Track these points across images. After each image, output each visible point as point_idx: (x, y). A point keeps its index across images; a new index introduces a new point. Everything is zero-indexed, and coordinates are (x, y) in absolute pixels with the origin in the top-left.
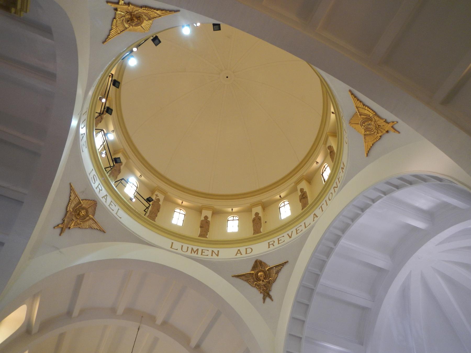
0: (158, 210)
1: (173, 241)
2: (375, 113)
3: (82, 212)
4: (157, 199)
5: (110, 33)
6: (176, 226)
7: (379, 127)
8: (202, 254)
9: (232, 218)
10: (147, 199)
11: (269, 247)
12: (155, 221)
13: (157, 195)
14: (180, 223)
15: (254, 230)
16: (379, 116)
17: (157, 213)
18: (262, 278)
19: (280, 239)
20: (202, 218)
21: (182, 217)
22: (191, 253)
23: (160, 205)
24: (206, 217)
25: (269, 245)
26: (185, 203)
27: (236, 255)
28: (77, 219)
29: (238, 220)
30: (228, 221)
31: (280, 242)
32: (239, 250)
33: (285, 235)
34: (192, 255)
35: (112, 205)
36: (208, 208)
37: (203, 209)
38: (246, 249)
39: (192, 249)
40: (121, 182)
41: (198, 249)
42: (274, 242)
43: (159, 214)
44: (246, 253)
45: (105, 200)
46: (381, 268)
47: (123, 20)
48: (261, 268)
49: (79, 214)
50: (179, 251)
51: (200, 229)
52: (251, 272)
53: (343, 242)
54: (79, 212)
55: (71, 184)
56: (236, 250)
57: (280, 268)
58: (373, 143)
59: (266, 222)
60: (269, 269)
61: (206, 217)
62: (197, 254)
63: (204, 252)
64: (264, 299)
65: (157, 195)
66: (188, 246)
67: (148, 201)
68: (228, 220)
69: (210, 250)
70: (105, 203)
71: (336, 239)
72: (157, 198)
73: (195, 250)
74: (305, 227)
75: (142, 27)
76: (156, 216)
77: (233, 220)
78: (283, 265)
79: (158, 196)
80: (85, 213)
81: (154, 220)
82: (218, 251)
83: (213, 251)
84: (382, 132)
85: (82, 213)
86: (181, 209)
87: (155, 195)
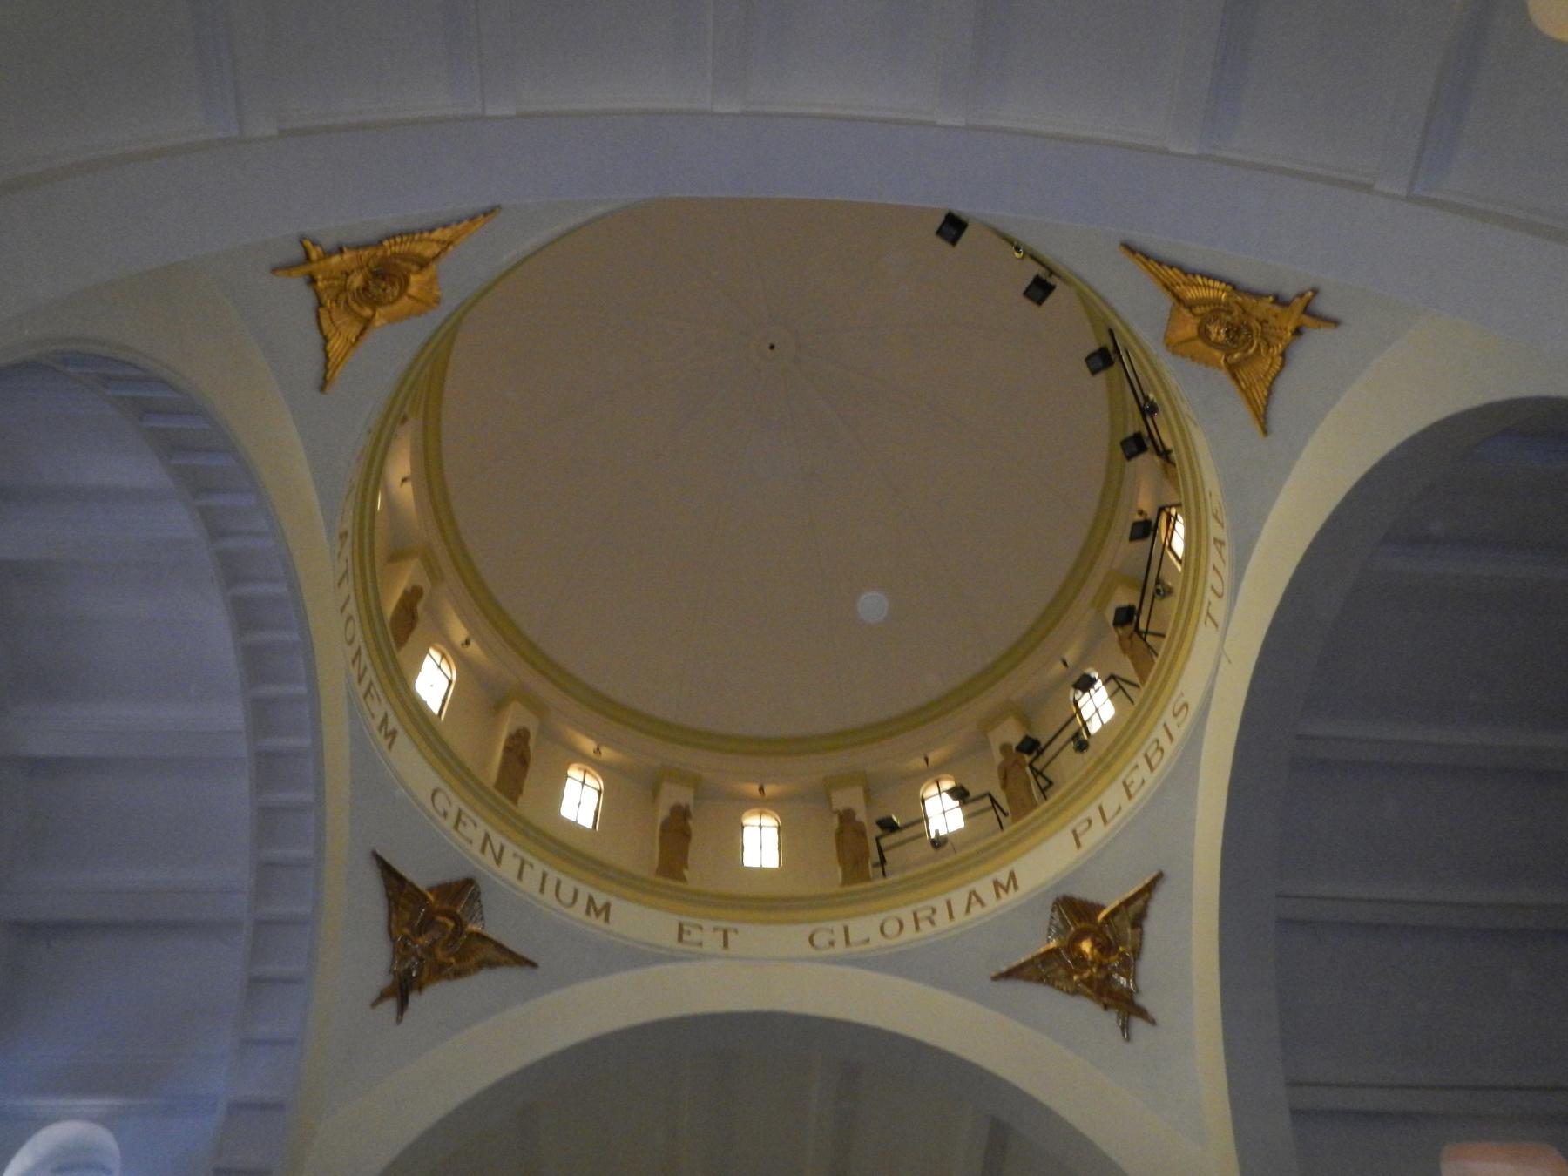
47: (347, 302)
75: (410, 297)
84: (1280, 339)
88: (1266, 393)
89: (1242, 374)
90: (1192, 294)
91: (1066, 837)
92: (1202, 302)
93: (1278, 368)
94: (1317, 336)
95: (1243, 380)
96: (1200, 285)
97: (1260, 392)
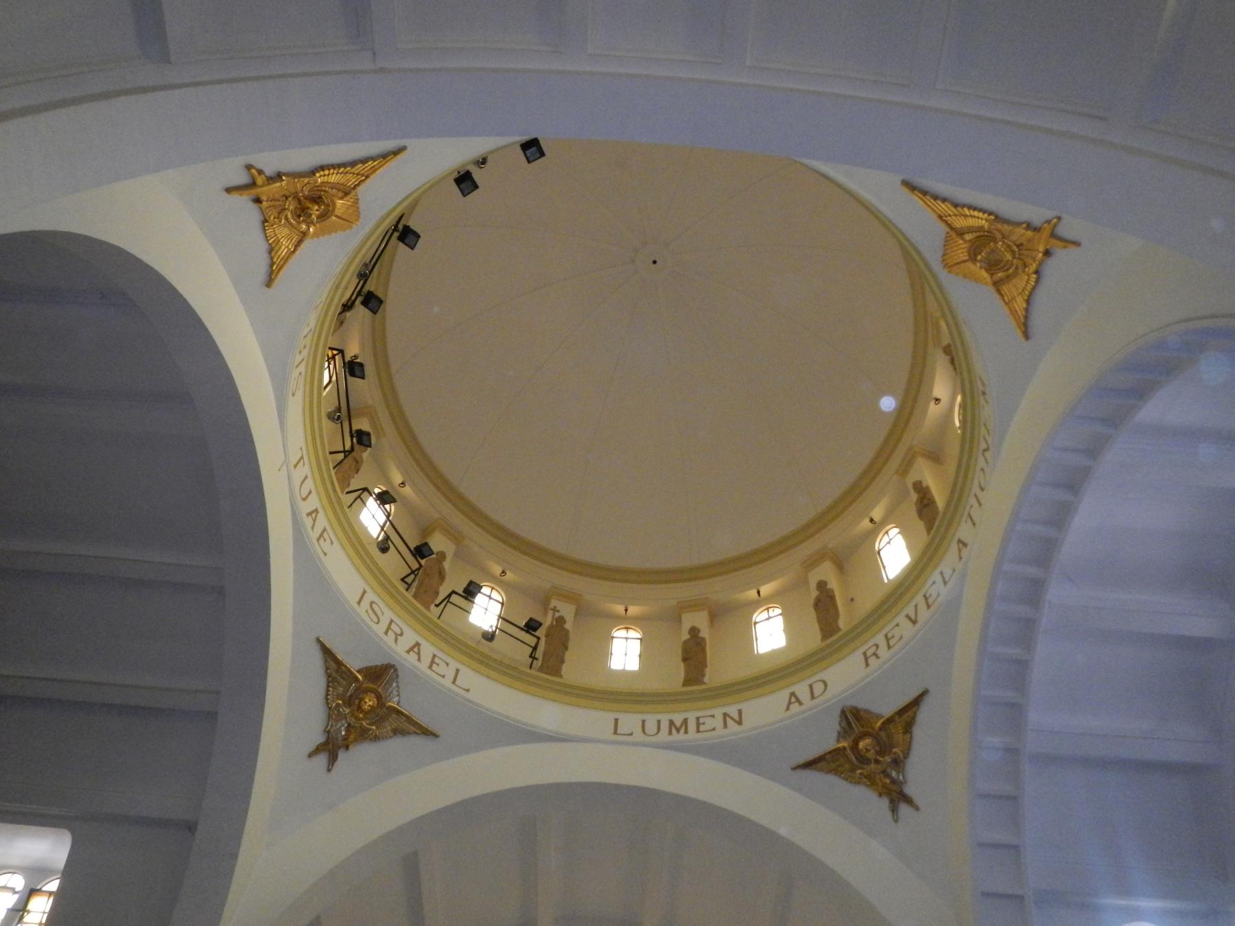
0: (563, 645)
1: (616, 715)
2: (992, 217)
3: (367, 700)
4: (556, 620)
5: (272, 258)
6: (624, 674)
7: (1021, 247)
8: (698, 731)
9: (764, 615)
10: (527, 625)
11: (867, 665)
12: (561, 676)
13: (555, 610)
14: (633, 664)
15: (822, 630)
16: (1007, 221)
17: (564, 653)
18: (871, 755)
19: (890, 636)
20: (685, 636)
21: (635, 647)
22: (670, 733)
23: (567, 632)
24: (694, 631)
25: (866, 659)
26: (633, 610)
27: (788, 708)
28: (360, 719)
29: (780, 614)
30: (757, 625)
31: (892, 642)
32: (793, 694)
33: (901, 619)
34: (671, 738)
35: (438, 665)
37: (684, 612)
38: (811, 686)
39: (671, 723)
40: (451, 603)
41: (685, 721)
42: (877, 646)
43: (568, 656)
44: (813, 697)
45: (416, 657)
46: (1207, 640)
48: (863, 726)
49: (359, 708)
50: (639, 736)
51: (682, 664)
52: (839, 746)
53: (1057, 593)
54: (360, 703)
55: (321, 639)
56: (784, 695)
57: (910, 713)
58: (1026, 298)
59: (852, 600)
60: (883, 724)
62: (686, 732)
63: (704, 723)
64: (894, 810)
65: (555, 607)
66: (659, 717)
67: (530, 631)
68: (755, 623)
69: (719, 713)
70: (417, 663)
71: (1034, 591)
72: (557, 615)
73: (678, 724)
74: (945, 583)
76: (562, 661)
77: (770, 618)
78: (916, 702)
79: (558, 611)
80: (375, 700)
81: (556, 672)
82: (740, 712)
83: (725, 715)
85: (366, 703)
87: (552, 609)
90: (960, 223)
91: (857, 657)
92: (970, 230)
94: (1062, 256)
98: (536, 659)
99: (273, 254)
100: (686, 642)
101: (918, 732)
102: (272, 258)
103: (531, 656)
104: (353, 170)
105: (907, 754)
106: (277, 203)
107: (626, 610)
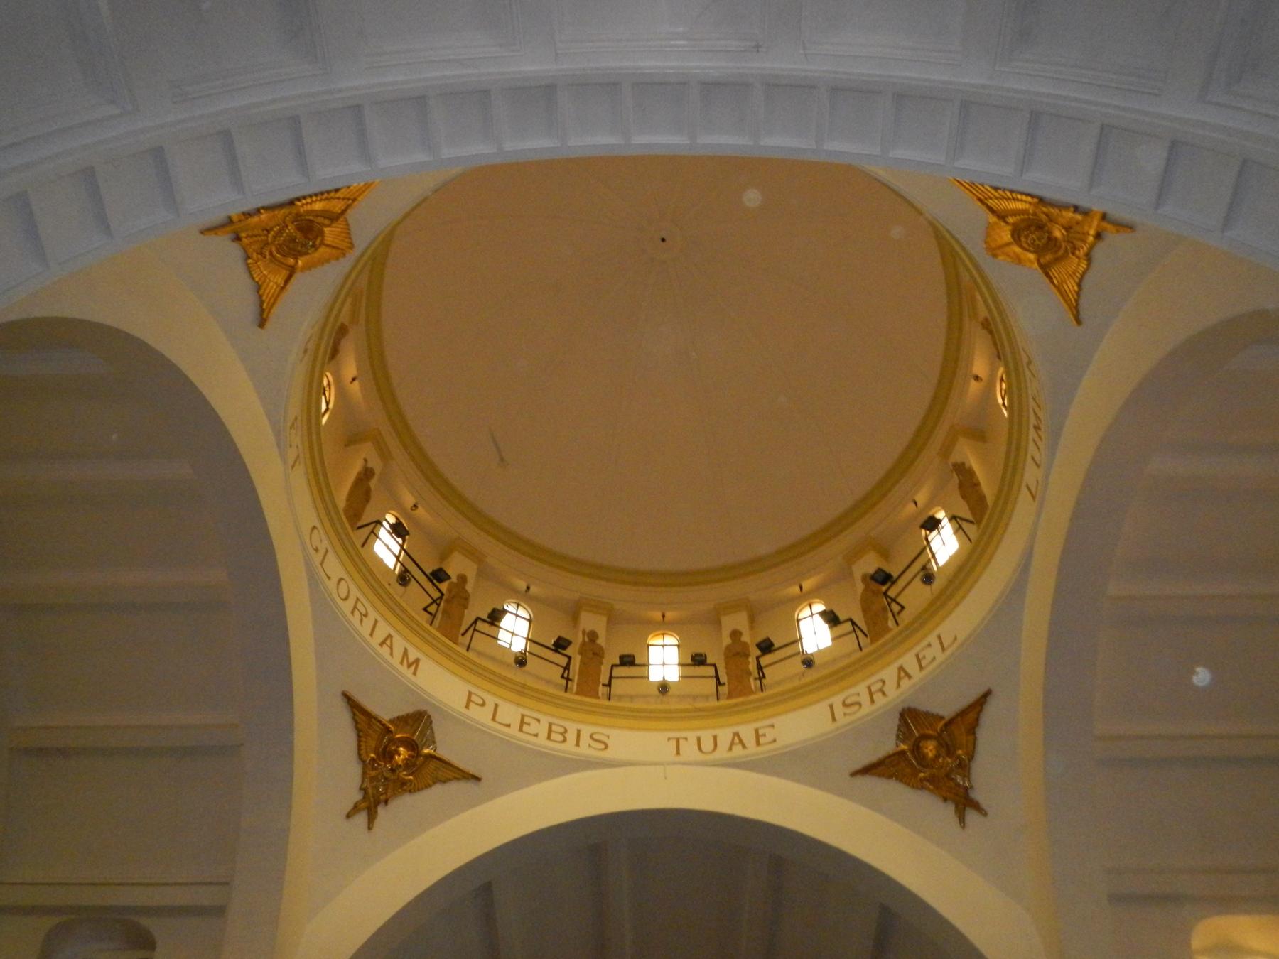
5: (260, 297)
36: (733, 607)
47: (271, 253)
61: (736, 634)
75: (328, 246)
86: (663, 634)
88: (1076, 288)
89: (1054, 272)
93: (1085, 266)
95: (1055, 277)
96: (1009, 199)
97: (1071, 286)
98: (571, 680)
99: (261, 293)
100: (728, 648)
101: (983, 734)
102: (260, 297)
103: (562, 677)
104: (337, 195)
105: (971, 757)
106: (259, 238)
107: (663, 616)
